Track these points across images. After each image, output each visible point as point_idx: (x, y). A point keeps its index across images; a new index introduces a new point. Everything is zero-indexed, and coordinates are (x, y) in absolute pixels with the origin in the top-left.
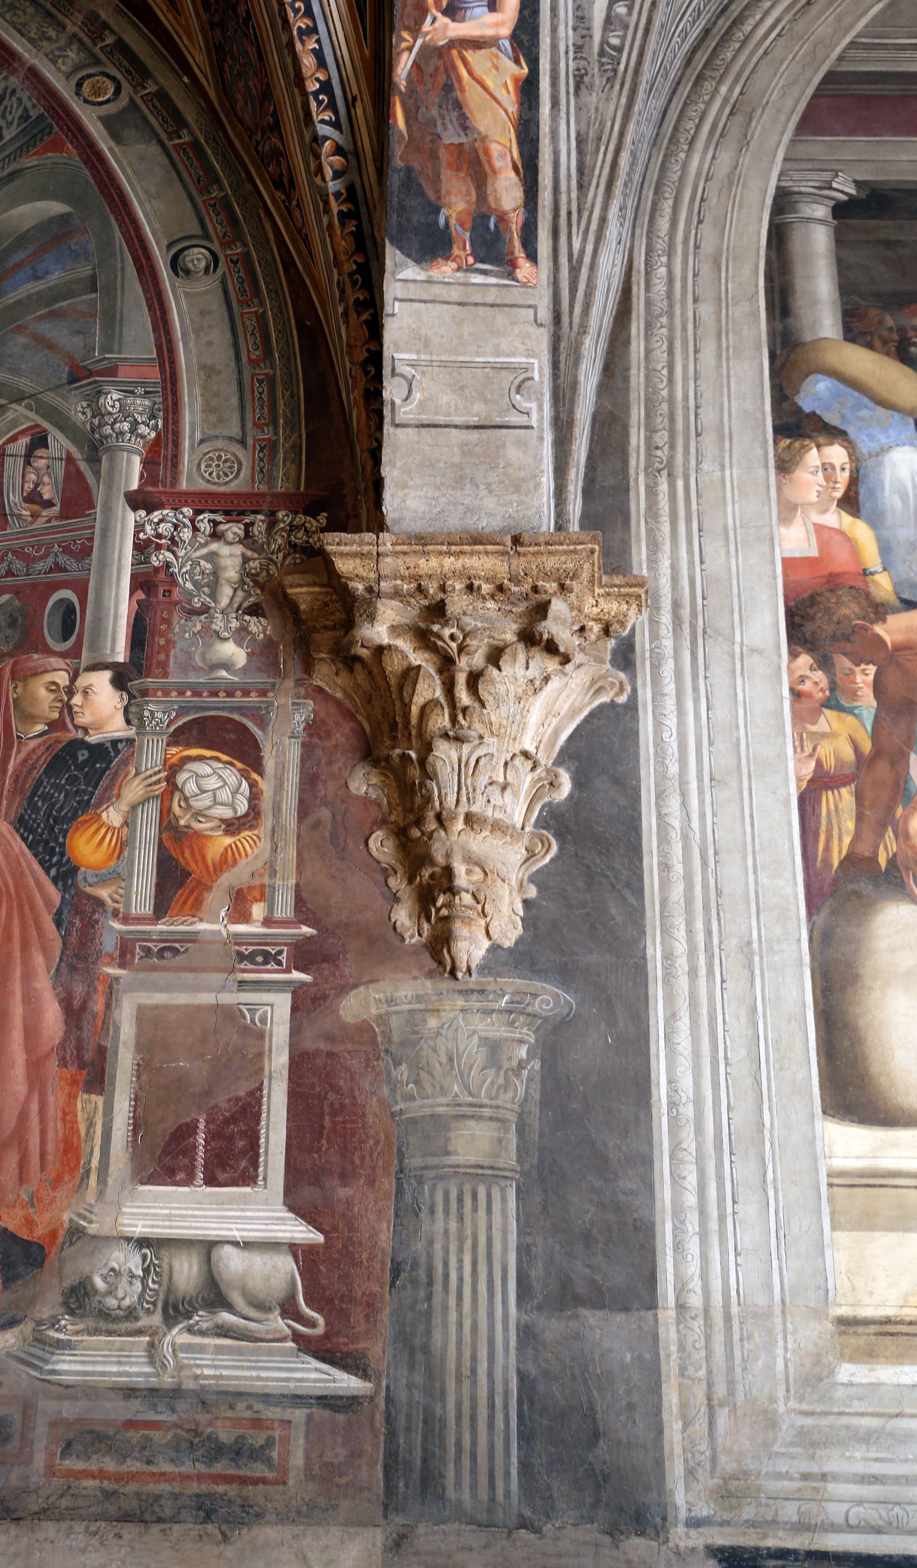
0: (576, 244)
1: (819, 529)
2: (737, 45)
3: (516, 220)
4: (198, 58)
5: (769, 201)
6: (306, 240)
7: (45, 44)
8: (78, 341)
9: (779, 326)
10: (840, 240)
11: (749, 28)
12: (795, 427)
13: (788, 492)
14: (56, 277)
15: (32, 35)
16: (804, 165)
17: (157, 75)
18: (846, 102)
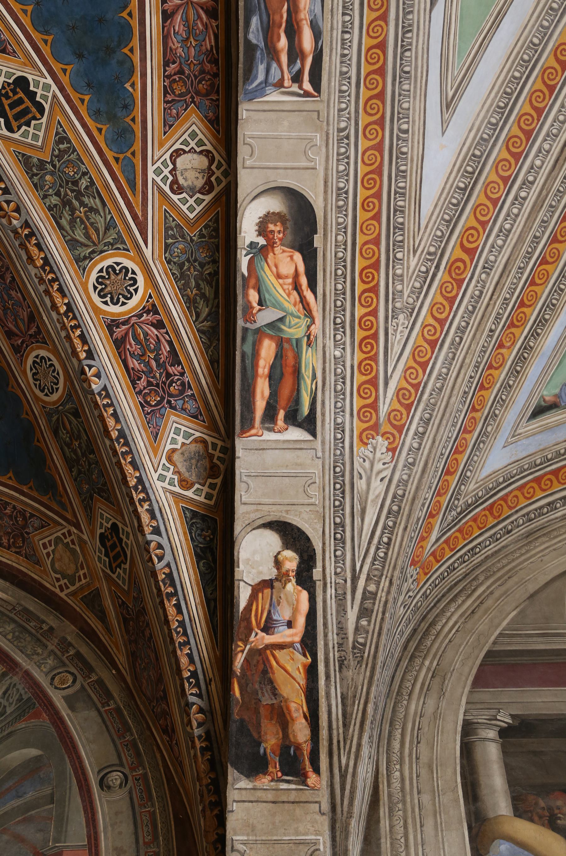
0: (344, 761)
2: (433, 637)
3: (306, 749)
4: (121, 660)
5: (459, 729)
6: (181, 764)
7: (35, 657)
8: (39, 836)
9: (472, 808)
10: (505, 752)
11: (440, 627)
14: (30, 795)
15: (28, 652)
16: (479, 706)
17: (97, 670)
18: (499, 668)
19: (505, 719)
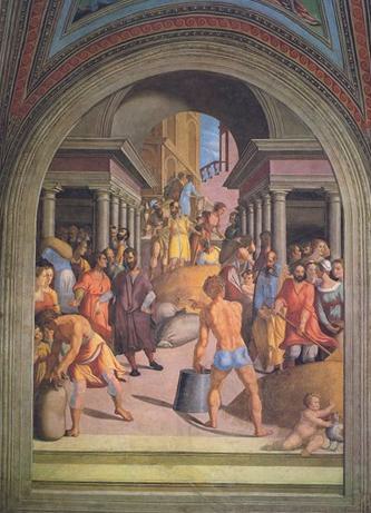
10: (56, 206)
12: (42, 263)
18: (64, 158)
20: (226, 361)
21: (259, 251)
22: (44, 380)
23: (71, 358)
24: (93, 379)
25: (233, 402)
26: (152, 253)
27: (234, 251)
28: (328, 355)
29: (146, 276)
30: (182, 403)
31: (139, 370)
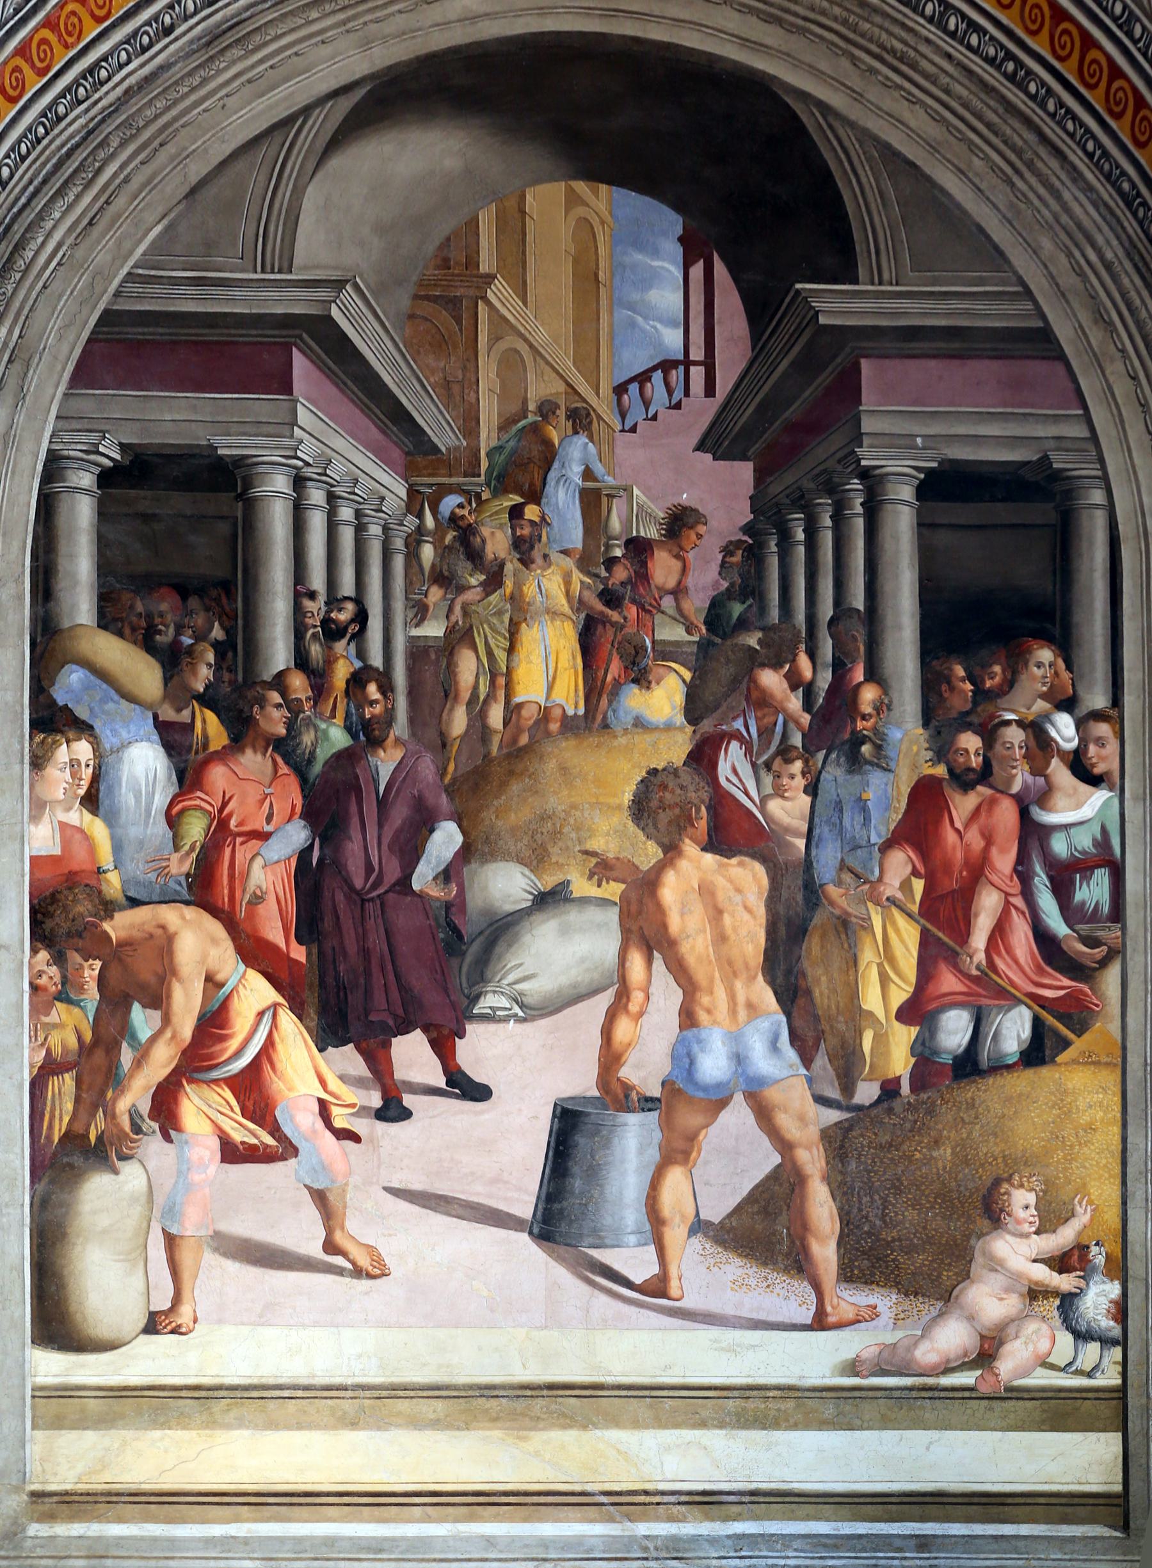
1: (63, 826)
2: (18, 276)
10: (103, 514)
11: (30, 254)
12: (51, 720)
13: (38, 788)
16: (75, 425)
19: (111, 452)
20: (713, 1065)
21: (825, 679)
22: (67, 1137)
23: (162, 1060)
24: (243, 1132)
25: (738, 1210)
26: (448, 692)
27: (735, 682)
28: (1066, 1044)
29: (427, 767)
30: (559, 1216)
31: (408, 1100)
